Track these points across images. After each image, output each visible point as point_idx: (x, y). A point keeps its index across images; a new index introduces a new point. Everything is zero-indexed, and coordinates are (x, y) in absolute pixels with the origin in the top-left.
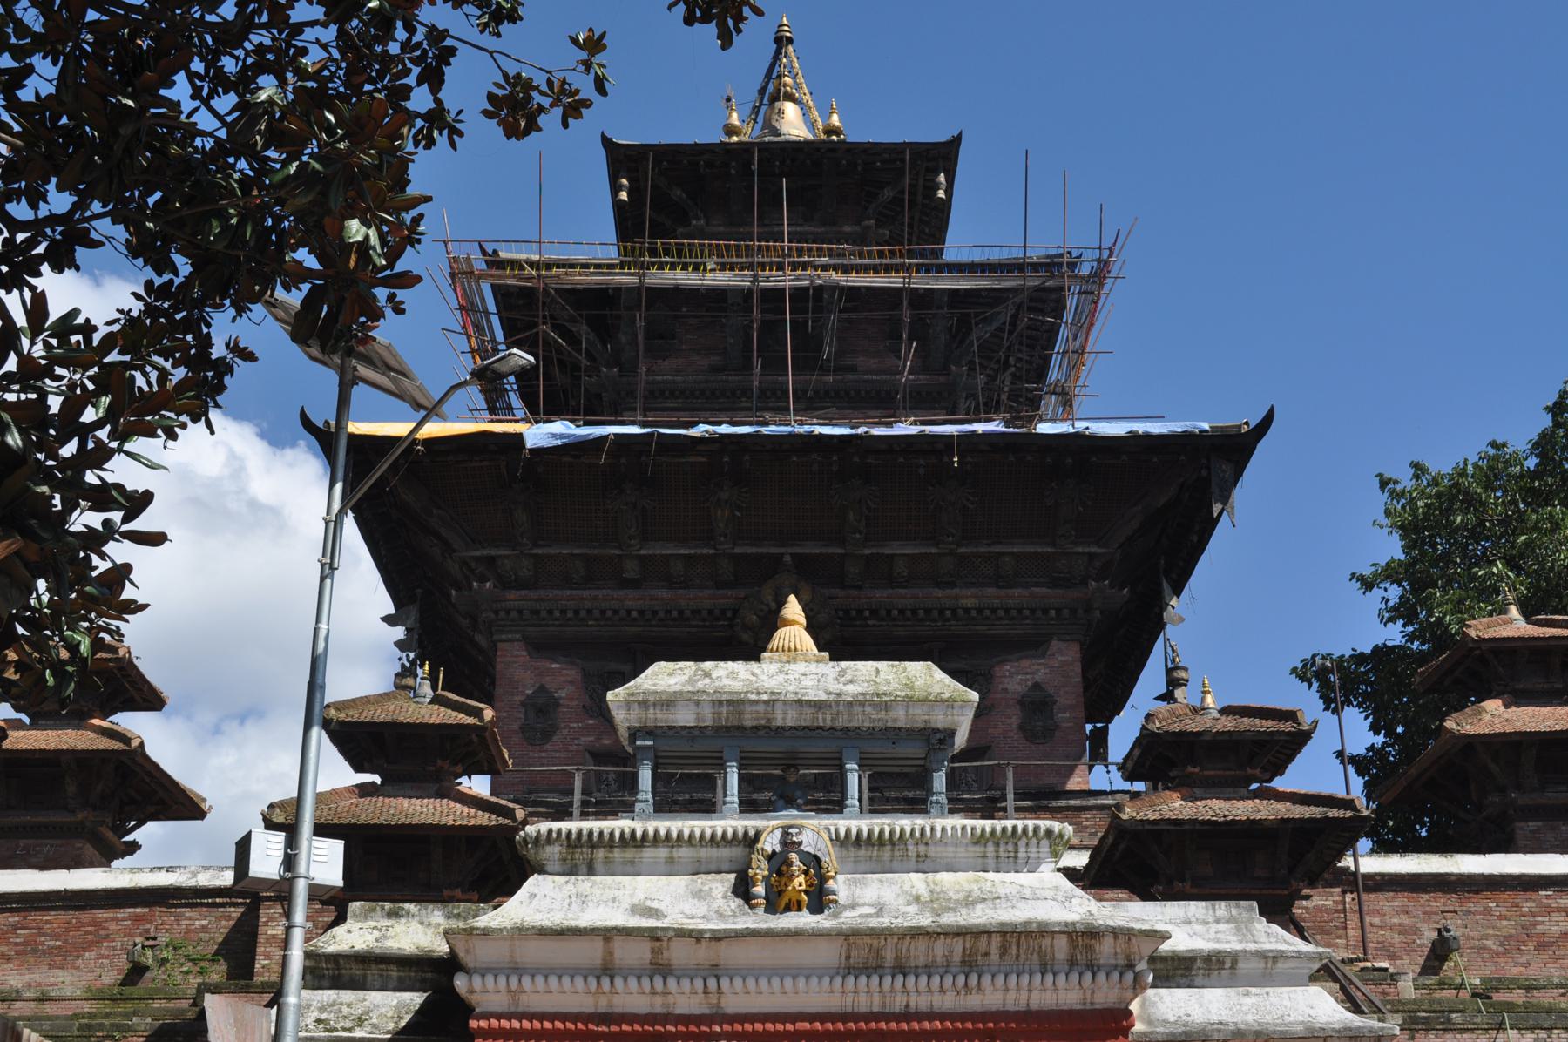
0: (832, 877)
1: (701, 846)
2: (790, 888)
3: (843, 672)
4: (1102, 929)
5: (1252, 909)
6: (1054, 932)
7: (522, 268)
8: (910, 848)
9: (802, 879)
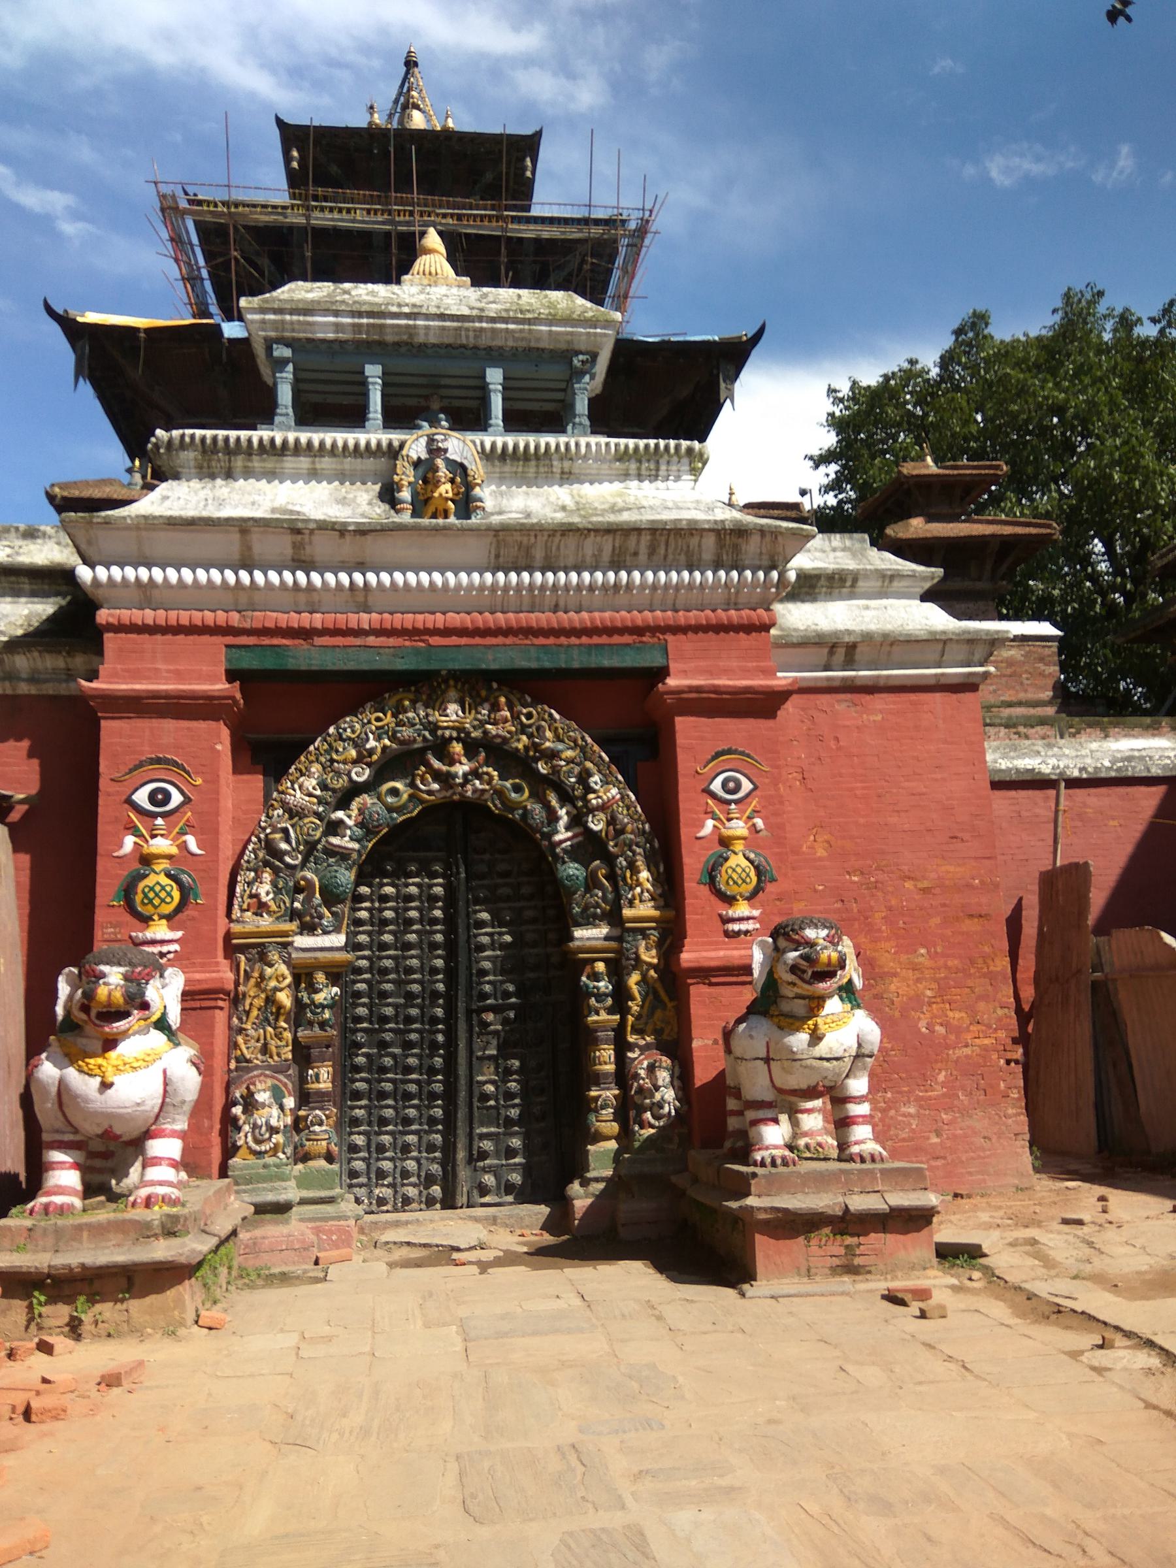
0: (479, 485)
1: (345, 456)
2: (436, 495)
3: (485, 295)
4: (751, 526)
5: (864, 541)
6: (704, 530)
7: (216, 206)
8: (555, 463)
9: (448, 486)
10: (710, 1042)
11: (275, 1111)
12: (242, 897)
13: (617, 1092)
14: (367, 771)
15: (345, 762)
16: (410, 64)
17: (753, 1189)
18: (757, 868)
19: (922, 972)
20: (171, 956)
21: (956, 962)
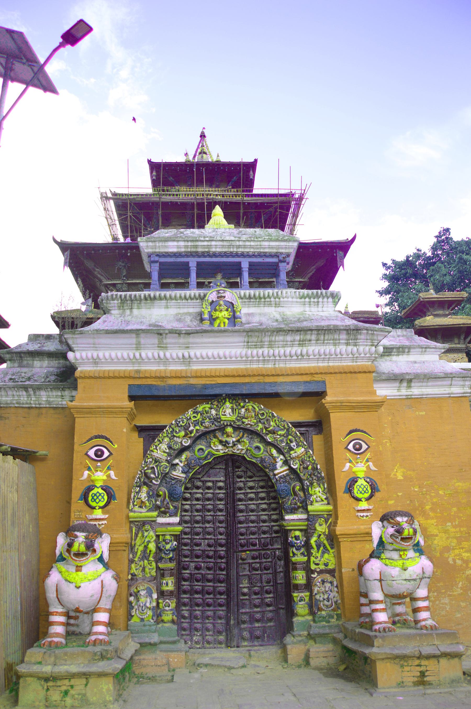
6: (341, 330)
10: (351, 570)
11: (148, 600)
12: (134, 499)
13: (308, 594)
14: (189, 441)
15: (179, 437)
16: (203, 136)
17: (375, 644)
18: (370, 485)
19: (449, 534)
20: (103, 526)
21: (465, 529)
